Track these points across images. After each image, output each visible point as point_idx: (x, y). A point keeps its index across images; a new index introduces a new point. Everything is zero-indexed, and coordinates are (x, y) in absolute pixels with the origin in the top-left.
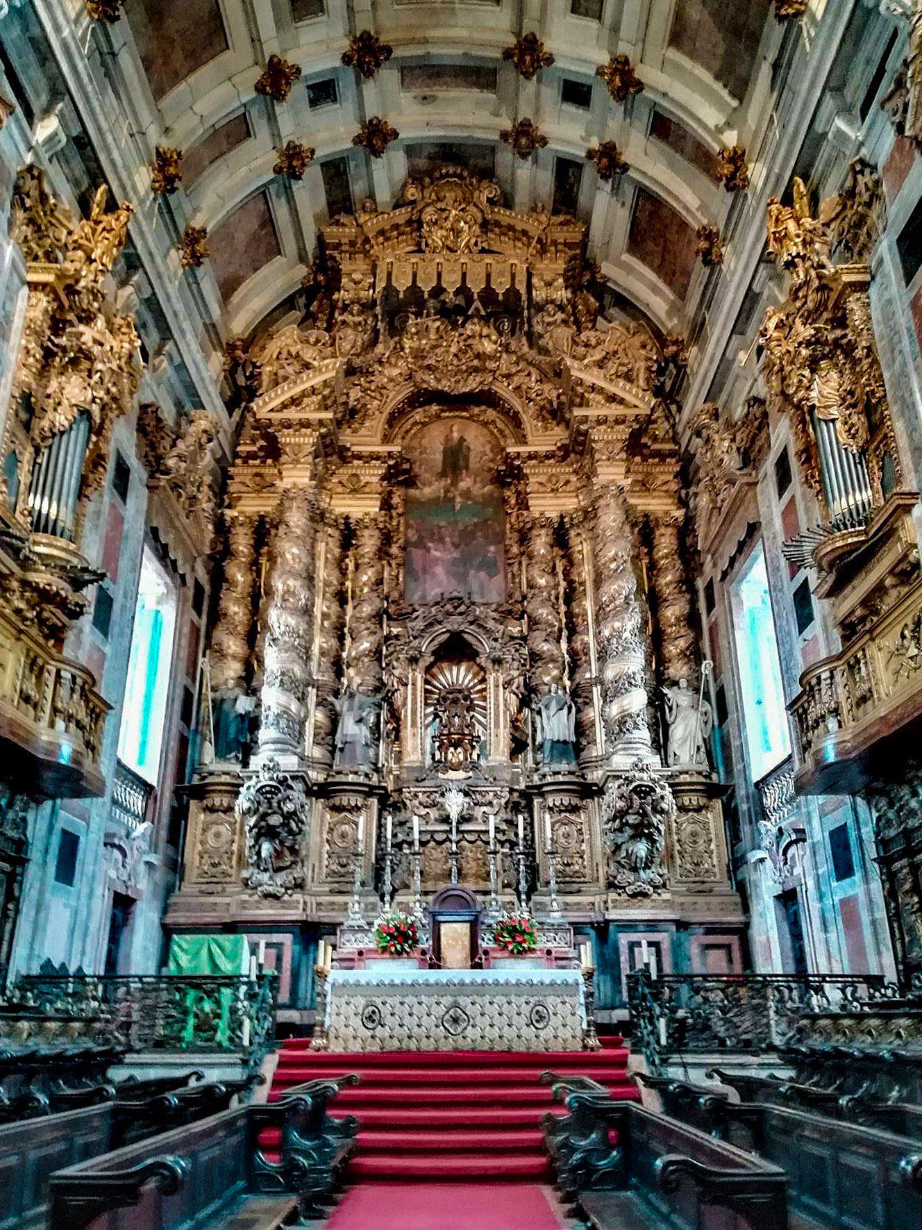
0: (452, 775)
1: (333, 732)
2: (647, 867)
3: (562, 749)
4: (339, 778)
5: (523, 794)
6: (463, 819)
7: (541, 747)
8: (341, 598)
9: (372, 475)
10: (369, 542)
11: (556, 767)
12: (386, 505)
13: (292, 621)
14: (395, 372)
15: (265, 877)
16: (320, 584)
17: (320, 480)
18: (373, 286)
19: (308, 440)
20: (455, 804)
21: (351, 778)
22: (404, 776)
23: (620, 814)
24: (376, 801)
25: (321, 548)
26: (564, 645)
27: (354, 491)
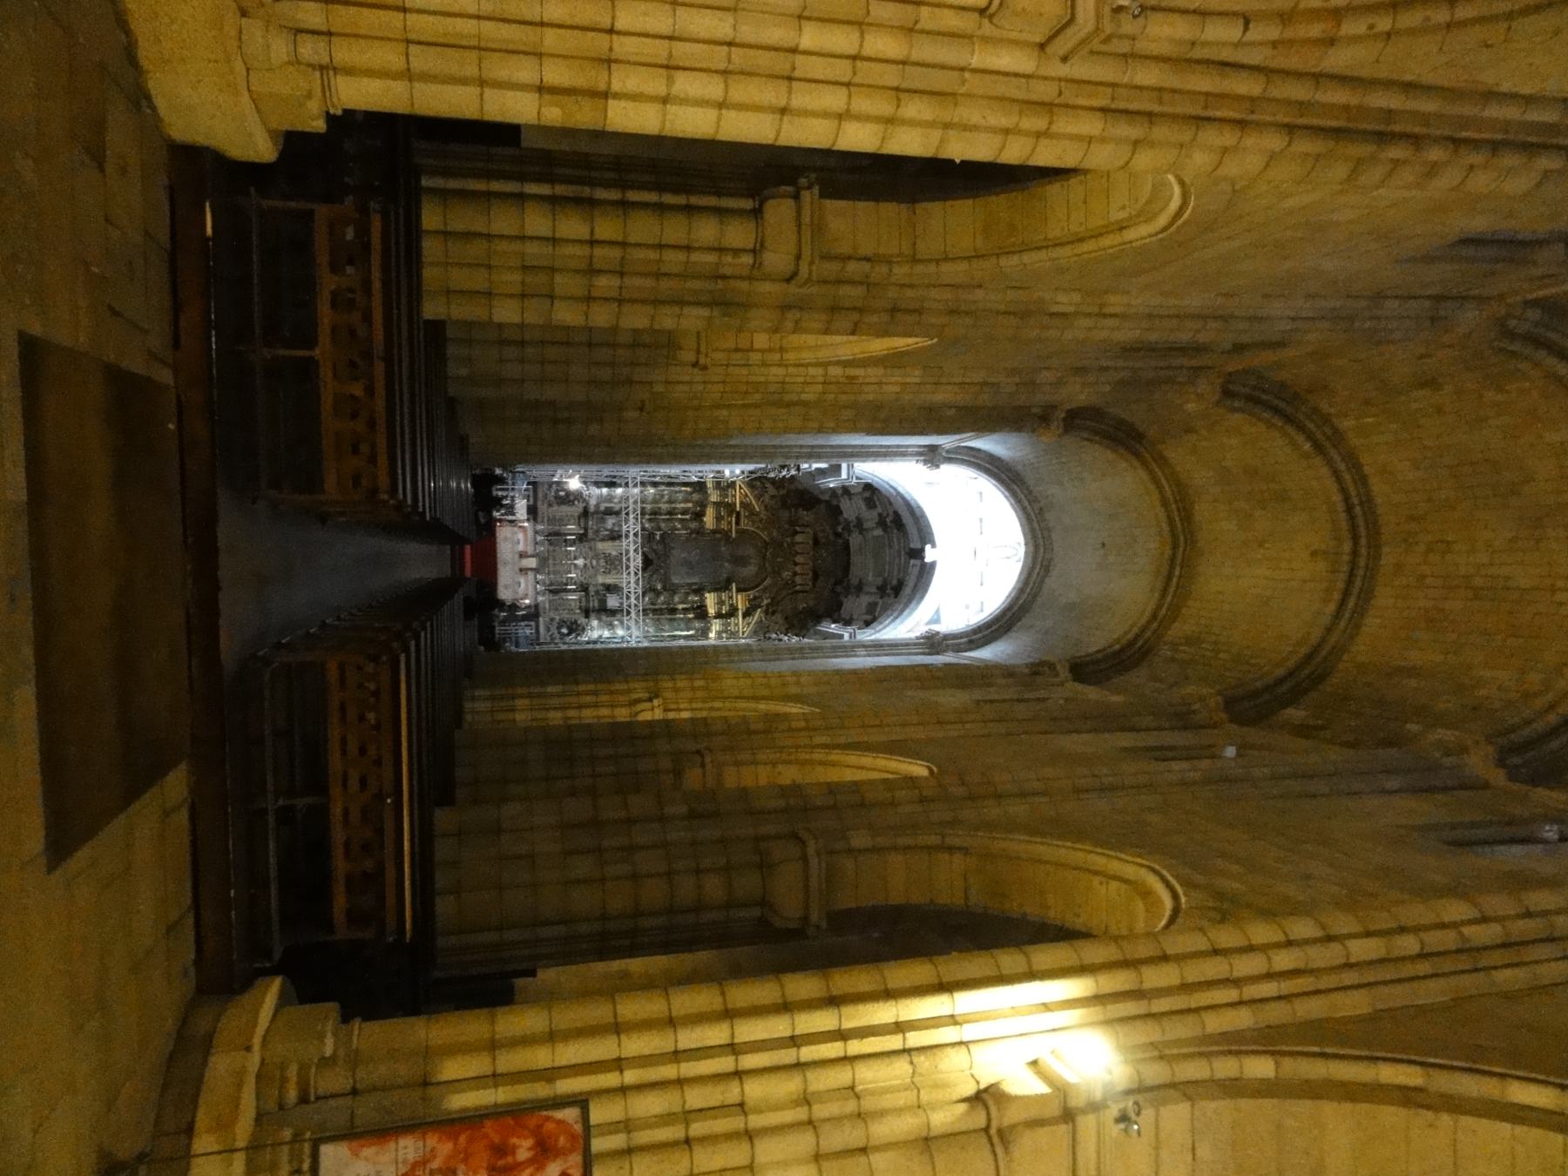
0: (594, 562)
1: (611, 514)
2: (559, 633)
3: (603, 602)
4: (590, 518)
5: (587, 588)
6: (575, 565)
7: (605, 595)
8: (670, 513)
9: (724, 525)
10: (694, 525)
11: (596, 601)
12: (714, 532)
13: (651, 498)
14: (774, 534)
15: (553, 494)
16: (673, 505)
17: (717, 505)
18: (803, 525)
19: (729, 500)
20: (580, 562)
21: (590, 523)
22: (593, 542)
23: (576, 621)
24: (582, 532)
25: (690, 505)
26: (652, 607)
27: (717, 518)
